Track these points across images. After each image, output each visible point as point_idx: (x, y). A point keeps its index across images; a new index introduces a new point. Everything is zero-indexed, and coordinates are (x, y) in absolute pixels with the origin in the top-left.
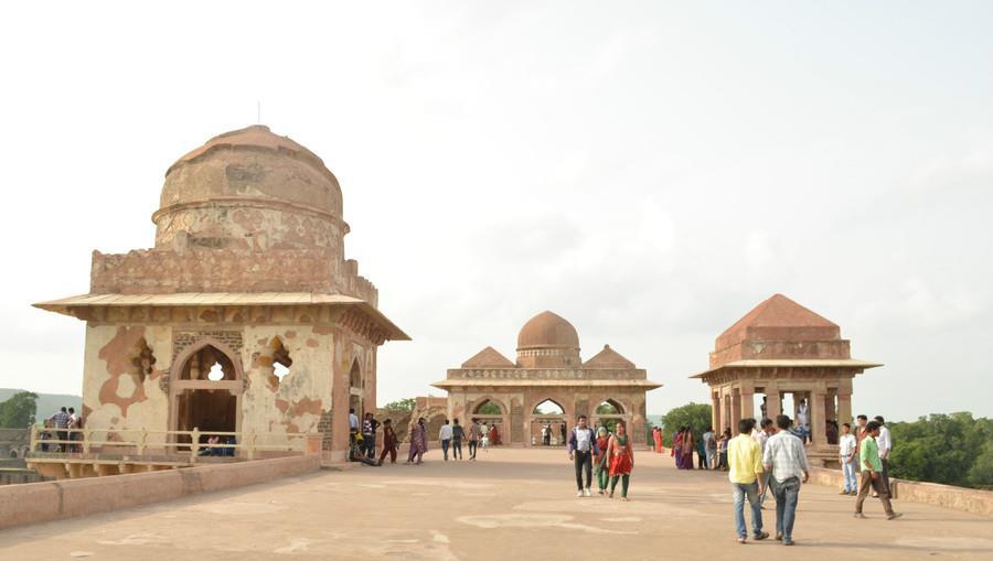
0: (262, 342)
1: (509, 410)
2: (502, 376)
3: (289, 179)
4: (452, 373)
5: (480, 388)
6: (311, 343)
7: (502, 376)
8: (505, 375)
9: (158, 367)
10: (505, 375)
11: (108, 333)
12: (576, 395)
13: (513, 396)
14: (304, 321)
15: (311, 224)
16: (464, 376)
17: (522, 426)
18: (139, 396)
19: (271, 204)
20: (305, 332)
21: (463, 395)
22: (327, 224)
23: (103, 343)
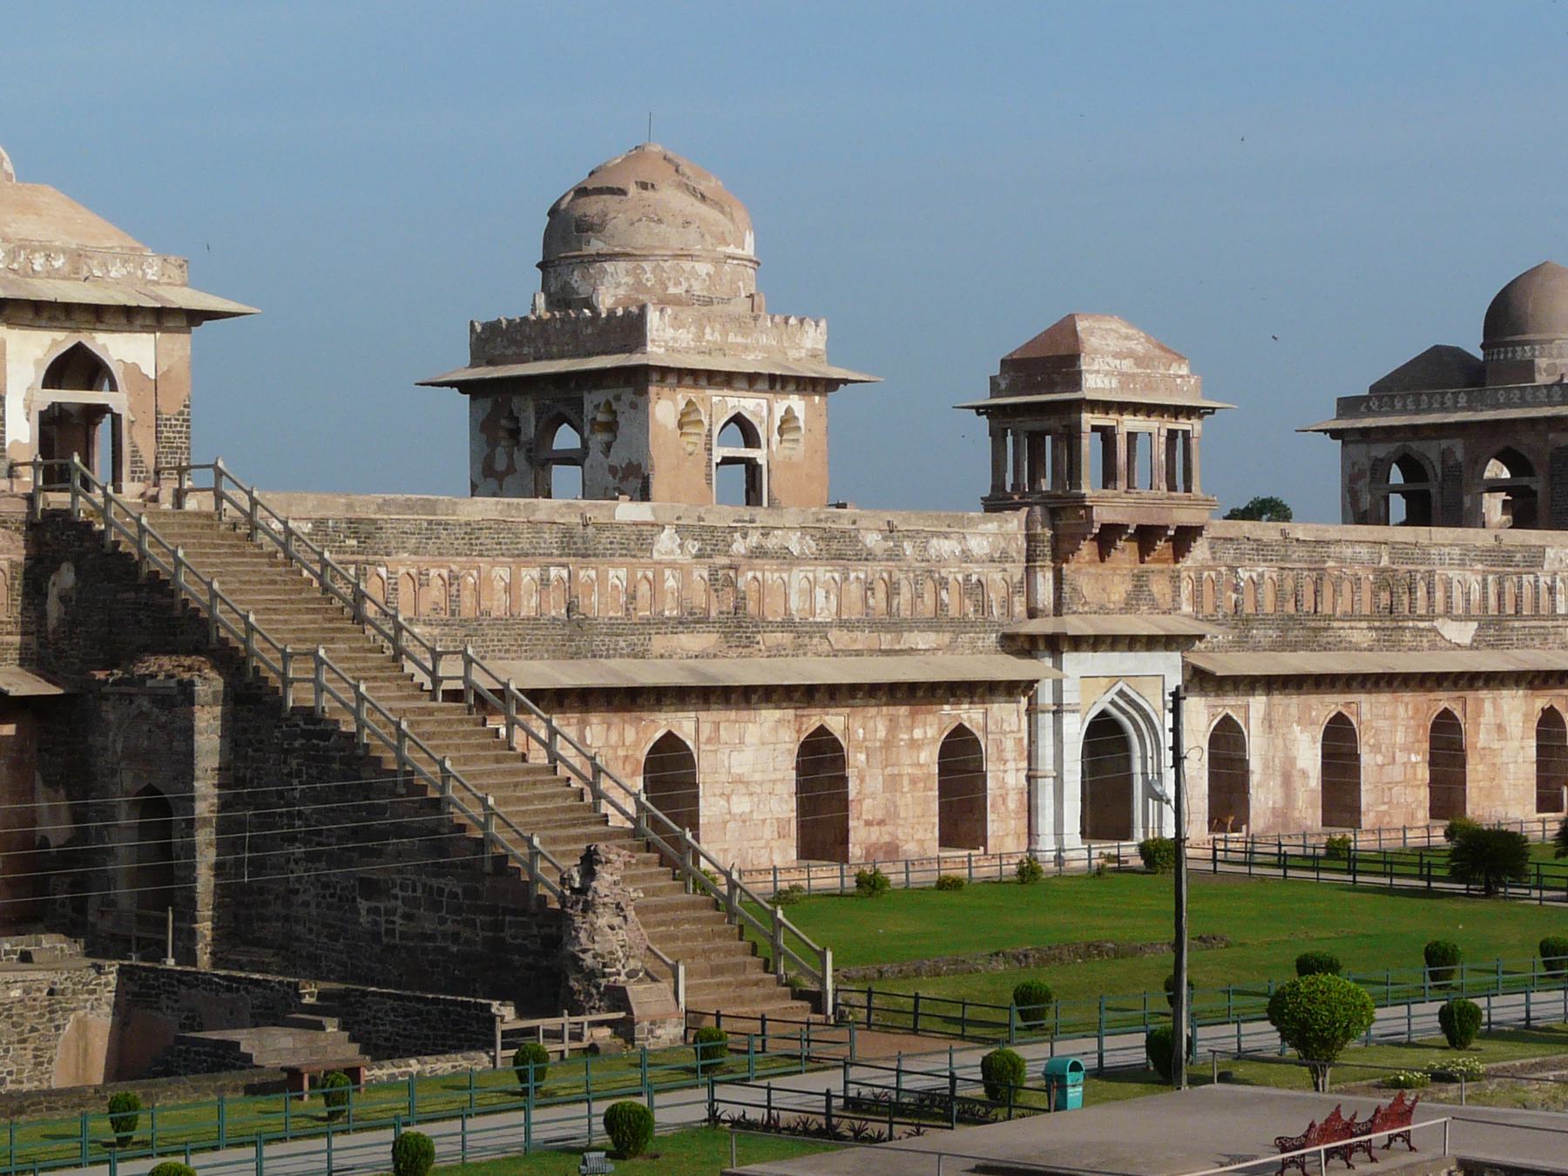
0: (597, 407)
1: (1439, 471)
2: (1449, 404)
3: (632, 224)
4: (1348, 406)
5: (1390, 432)
6: (634, 406)
7: (1436, 405)
8: (1430, 404)
9: (523, 438)
10: (1430, 404)
11: (487, 404)
12: (1551, 436)
13: (1444, 444)
14: (628, 383)
15: (663, 270)
16: (1363, 409)
17: (1461, 503)
18: (511, 469)
19: (612, 257)
20: (628, 394)
21: (1362, 448)
22: (687, 265)
23: (482, 416)
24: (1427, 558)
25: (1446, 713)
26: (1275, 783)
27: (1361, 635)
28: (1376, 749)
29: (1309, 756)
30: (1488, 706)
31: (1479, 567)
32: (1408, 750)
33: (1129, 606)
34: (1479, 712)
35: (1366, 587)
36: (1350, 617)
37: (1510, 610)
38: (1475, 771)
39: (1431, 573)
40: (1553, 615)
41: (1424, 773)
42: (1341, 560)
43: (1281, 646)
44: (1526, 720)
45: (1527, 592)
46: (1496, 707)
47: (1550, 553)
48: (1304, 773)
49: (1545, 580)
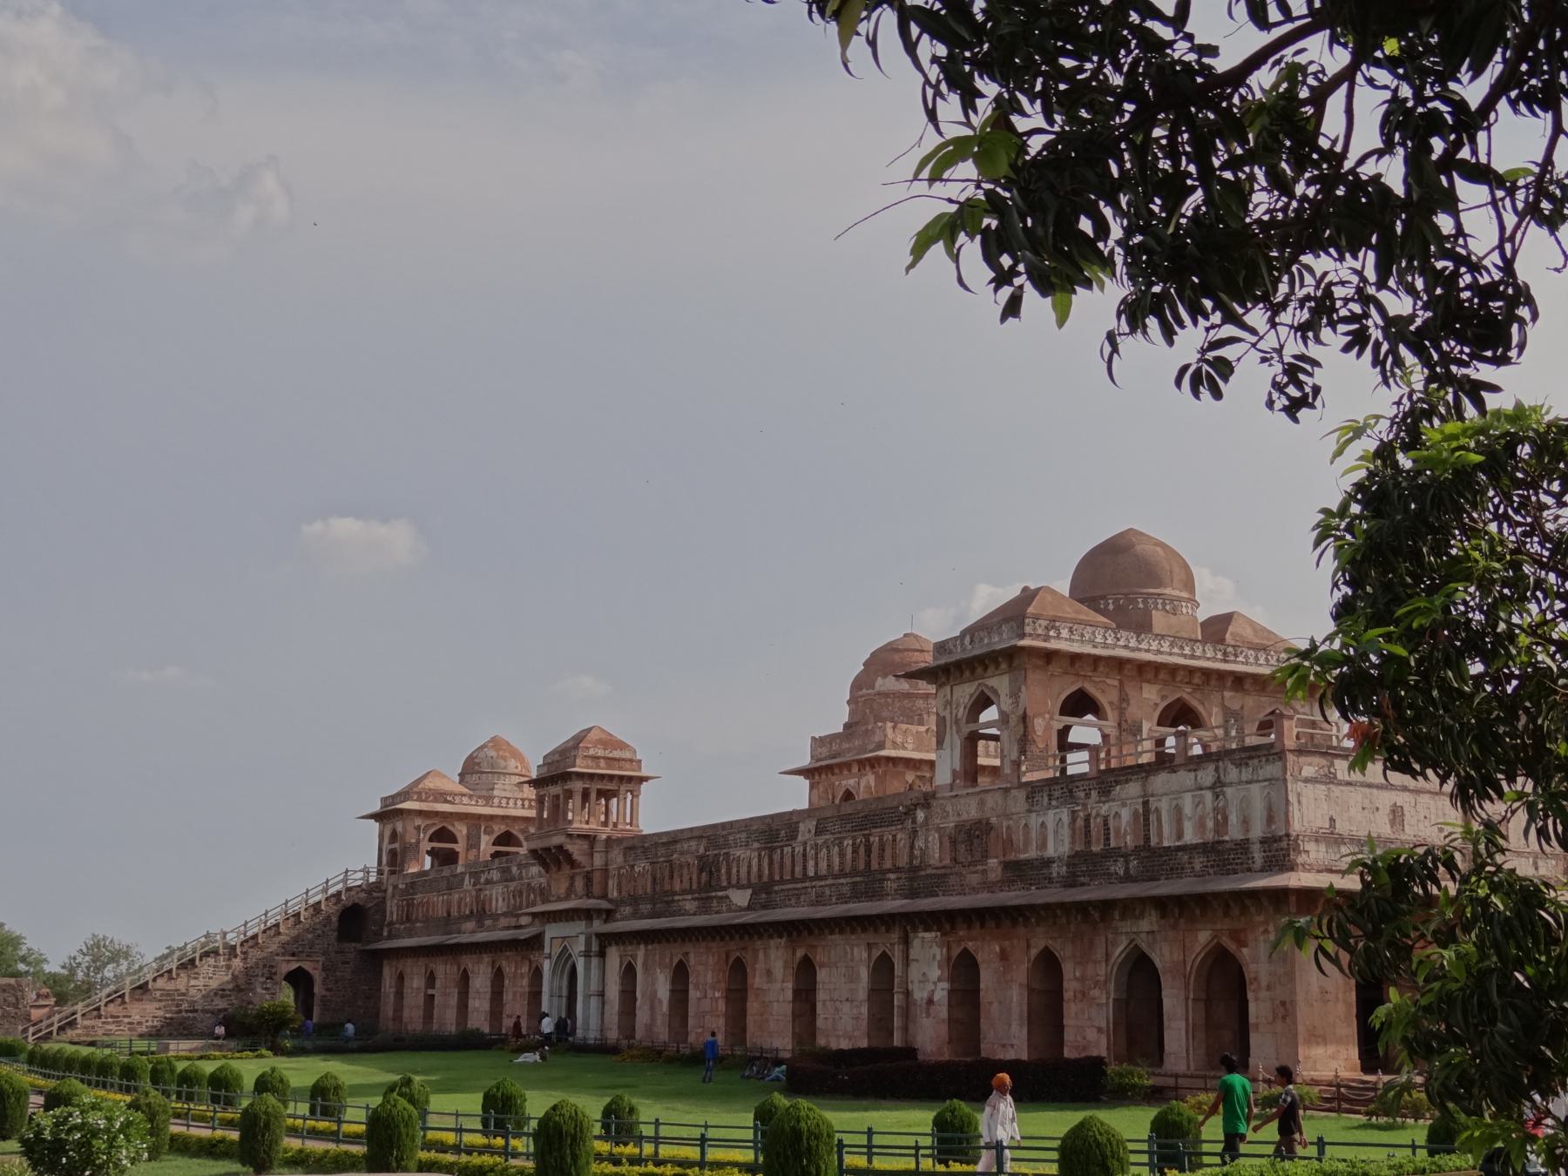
24: (727, 845)
25: (738, 961)
26: (646, 1007)
27: (690, 906)
28: (697, 987)
29: (663, 991)
30: (761, 956)
31: (756, 845)
32: (714, 989)
33: (567, 898)
34: (756, 960)
35: (695, 871)
36: (684, 892)
37: (777, 878)
38: (753, 1006)
39: (727, 854)
40: (805, 877)
41: (722, 1006)
42: (682, 853)
43: (654, 915)
44: (785, 968)
45: (788, 861)
46: (766, 955)
47: (802, 827)
48: (661, 1002)
49: (799, 849)
